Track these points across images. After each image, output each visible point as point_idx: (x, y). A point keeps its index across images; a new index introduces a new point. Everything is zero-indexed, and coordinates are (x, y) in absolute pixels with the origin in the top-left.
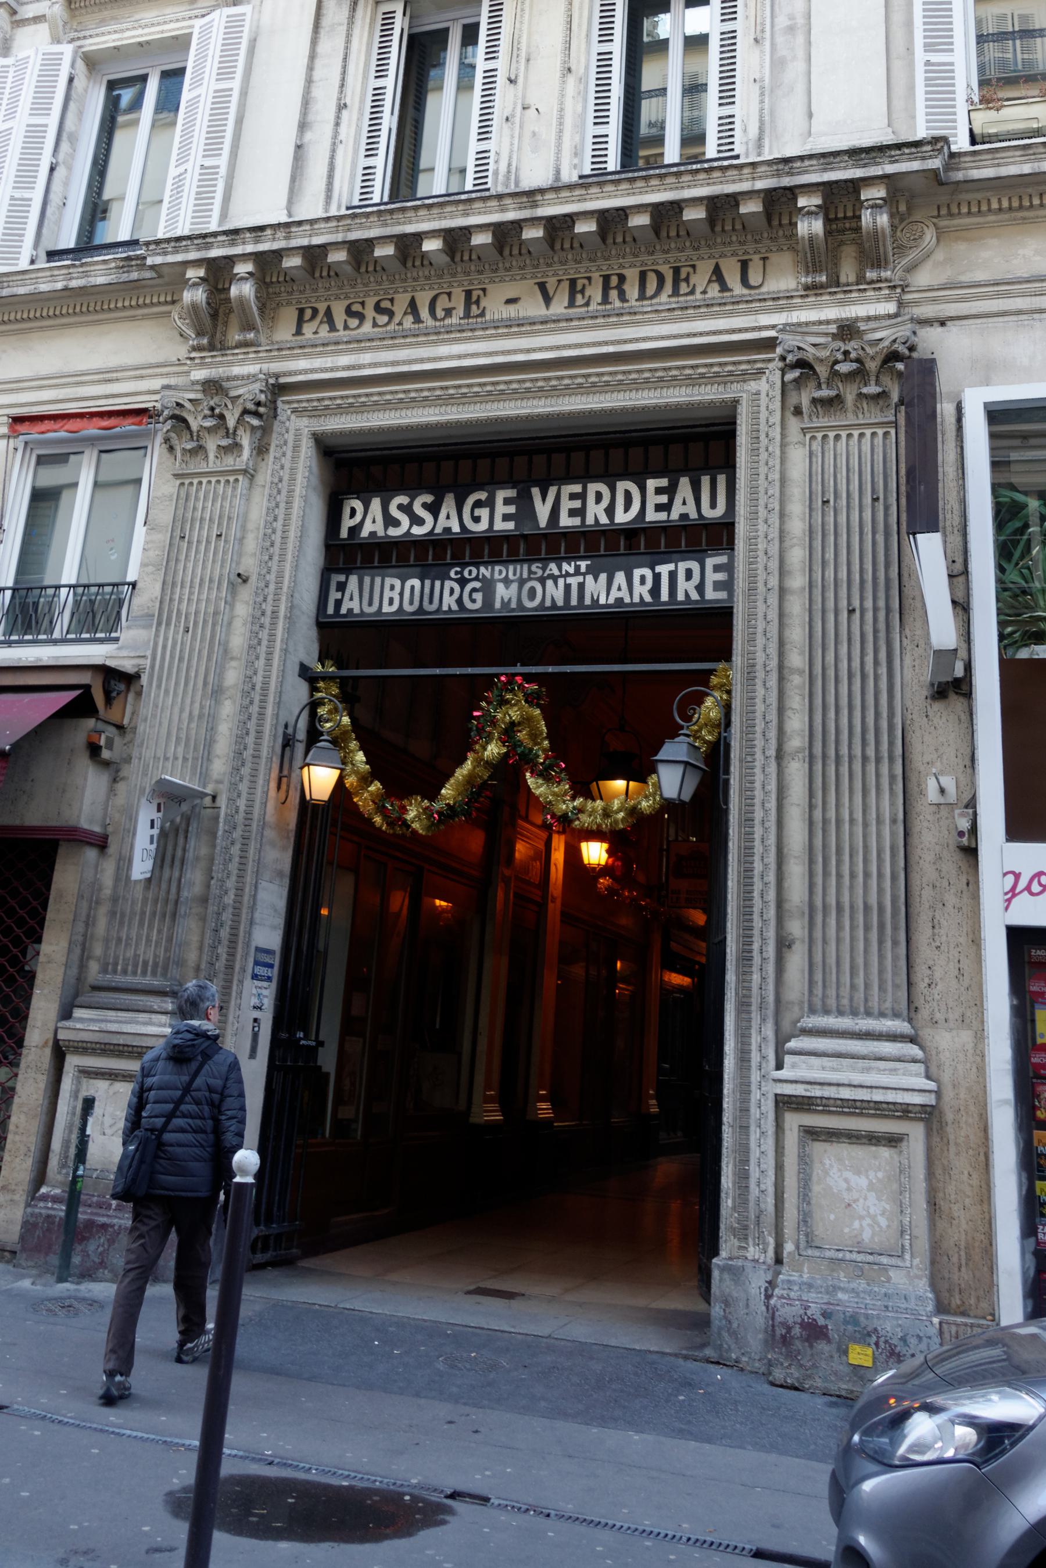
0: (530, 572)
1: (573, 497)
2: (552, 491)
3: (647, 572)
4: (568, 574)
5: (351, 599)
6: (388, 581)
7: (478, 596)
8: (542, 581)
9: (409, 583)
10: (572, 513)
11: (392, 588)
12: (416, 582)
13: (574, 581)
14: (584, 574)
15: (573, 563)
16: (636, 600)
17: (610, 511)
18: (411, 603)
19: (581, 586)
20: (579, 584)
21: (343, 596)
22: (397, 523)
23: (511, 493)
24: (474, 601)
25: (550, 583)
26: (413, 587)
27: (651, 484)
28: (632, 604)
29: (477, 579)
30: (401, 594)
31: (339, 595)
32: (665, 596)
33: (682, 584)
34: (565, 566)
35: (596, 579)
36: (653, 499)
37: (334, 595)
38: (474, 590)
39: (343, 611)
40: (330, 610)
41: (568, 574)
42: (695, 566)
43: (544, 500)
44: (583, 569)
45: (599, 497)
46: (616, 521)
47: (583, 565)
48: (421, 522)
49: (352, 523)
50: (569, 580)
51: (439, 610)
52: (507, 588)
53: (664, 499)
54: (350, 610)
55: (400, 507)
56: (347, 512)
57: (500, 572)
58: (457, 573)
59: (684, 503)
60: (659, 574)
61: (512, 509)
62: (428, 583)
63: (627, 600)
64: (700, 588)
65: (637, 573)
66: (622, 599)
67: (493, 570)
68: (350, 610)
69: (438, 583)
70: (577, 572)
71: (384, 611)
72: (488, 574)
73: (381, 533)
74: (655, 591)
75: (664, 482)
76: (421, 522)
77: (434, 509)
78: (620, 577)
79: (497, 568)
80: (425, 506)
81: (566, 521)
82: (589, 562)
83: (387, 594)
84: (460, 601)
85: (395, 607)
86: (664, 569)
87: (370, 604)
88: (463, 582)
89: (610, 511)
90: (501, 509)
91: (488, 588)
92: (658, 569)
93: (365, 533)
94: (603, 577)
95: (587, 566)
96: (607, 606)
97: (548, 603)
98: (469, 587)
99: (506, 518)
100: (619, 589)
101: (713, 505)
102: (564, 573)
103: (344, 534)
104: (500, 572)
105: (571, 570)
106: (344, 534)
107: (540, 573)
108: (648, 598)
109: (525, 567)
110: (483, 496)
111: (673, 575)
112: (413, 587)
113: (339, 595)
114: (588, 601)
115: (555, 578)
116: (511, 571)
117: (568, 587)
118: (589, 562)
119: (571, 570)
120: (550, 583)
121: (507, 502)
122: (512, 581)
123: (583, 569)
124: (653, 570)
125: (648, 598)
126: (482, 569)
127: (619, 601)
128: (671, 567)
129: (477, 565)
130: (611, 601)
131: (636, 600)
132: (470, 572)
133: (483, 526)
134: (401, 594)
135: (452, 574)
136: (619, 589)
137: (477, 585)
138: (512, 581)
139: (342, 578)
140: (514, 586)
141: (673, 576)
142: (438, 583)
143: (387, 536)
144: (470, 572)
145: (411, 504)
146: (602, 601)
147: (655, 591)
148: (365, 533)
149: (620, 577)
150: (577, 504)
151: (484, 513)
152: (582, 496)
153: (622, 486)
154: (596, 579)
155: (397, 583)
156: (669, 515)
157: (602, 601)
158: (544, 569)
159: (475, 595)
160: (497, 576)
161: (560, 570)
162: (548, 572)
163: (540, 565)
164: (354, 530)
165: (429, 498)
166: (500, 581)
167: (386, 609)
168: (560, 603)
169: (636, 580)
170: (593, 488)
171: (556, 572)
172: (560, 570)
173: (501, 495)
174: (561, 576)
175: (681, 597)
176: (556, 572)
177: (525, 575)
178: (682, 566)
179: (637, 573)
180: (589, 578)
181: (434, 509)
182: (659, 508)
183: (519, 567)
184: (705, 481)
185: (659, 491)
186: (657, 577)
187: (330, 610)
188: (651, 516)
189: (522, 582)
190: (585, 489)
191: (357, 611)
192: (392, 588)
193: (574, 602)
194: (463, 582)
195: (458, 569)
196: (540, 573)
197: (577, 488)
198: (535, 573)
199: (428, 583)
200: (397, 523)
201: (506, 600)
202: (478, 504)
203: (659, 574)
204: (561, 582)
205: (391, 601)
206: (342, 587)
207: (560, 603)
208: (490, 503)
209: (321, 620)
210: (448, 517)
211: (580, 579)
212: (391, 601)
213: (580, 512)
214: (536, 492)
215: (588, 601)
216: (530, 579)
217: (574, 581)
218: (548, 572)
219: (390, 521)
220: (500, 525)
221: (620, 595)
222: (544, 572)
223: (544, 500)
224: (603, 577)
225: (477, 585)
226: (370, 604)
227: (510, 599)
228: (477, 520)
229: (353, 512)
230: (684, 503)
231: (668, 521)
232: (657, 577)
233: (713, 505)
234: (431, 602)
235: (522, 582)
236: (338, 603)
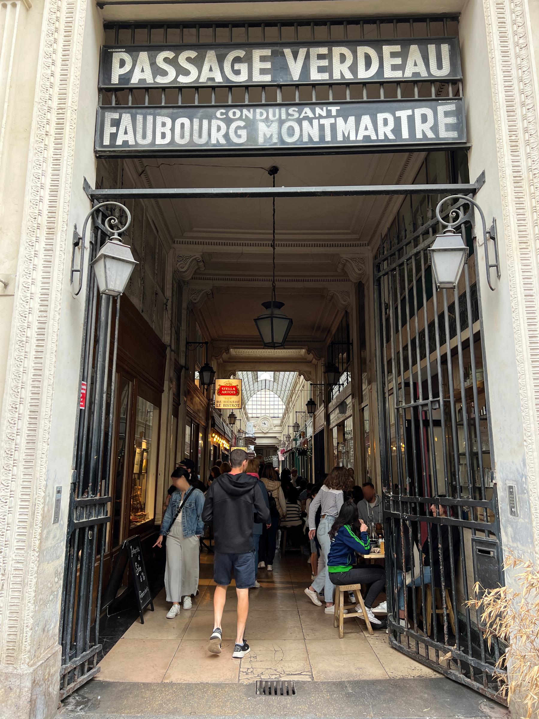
0: (288, 114)
1: (321, 57)
2: (302, 52)
3: (389, 117)
4: (321, 117)
5: (126, 133)
6: (160, 120)
7: (243, 133)
8: (299, 121)
9: (179, 122)
10: (321, 70)
11: (164, 124)
12: (186, 121)
13: (327, 122)
14: (335, 117)
15: (325, 108)
16: (381, 137)
17: (353, 69)
18: (182, 136)
19: (333, 127)
20: (331, 124)
21: (118, 130)
22: (164, 73)
23: (267, 52)
24: (239, 136)
25: (305, 123)
26: (183, 125)
27: (387, 49)
28: (378, 140)
29: (240, 119)
30: (173, 130)
31: (114, 130)
32: (405, 134)
33: (419, 127)
34: (318, 110)
35: (346, 121)
36: (388, 62)
37: (109, 130)
38: (239, 127)
39: (119, 142)
40: (107, 141)
41: (321, 117)
42: (429, 112)
43: (295, 57)
44: (334, 113)
45: (343, 58)
46: (359, 77)
47: (334, 109)
48: (187, 73)
49: (123, 71)
50: (322, 121)
51: (207, 144)
52: (268, 126)
53: (398, 61)
54: (125, 143)
55: (166, 60)
56: (116, 63)
57: (261, 114)
58: (222, 114)
59: (416, 65)
60: (400, 118)
61: (268, 65)
62: (196, 121)
63: (374, 137)
64: (435, 128)
65: (380, 117)
66: (369, 136)
67: (254, 112)
68: (125, 143)
69: (205, 122)
70: (329, 115)
71: (157, 143)
72: (250, 116)
73: (150, 80)
74: (397, 130)
75: (397, 48)
76: (187, 73)
77: (198, 62)
78: (366, 120)
79: (258, 110)
80: (189, 59)
81: (315, 76)
82: (339, 108)
83: (159, 130)
84: (226, 136)
85: (168, 140)
86: (404, 114)
87: (144, 137)
88: (228, 122)
89: (353, 69)
90: (257, 65)
91: (250, 125)
92: (398, 114)
93: (135, 80)
94: (352, 120)
95: (337, 110)
96: (356, 141)
97: (305, 139)
98: (233, 126)
99: (263, 71)
100: (366, 129)
101: (440, 66)
102: (317, 115)
103: (115, 80)
104: (261, 114)
105: (324, 114)
106: (115, 80)
107: (296, 115)
108: (391, 136)
109: (283, 110)
110: (241, 53)
111: (411, 119)
112: (183, 125)
113: (114, 130)
114: (340, 138)
115: (310, 120)
116: (272, 113)
117: (322, 128)
118: (339, 108)
119: (324, 114)
120: (305, 123)
121: (263, 59)
122: (272, 121)
123: (334, 113)
124: (394, 115)
125: (391, 136)
126: (245, 111)
127: (367, 138)
128: (409, 112)
129: (241, 106)
130: (360, 138)
131: (381, 137)
132: (234, 114)
133: (242, 78)
134: (173, 130)
135: (218, 114)
136: (366, 129)
137: (242, 124)
138: (272, 121)
139: (116, 116)
140: (275, 125)
141: (411, 119)
142: (205, 122)
143: (155, 83)
144: (234, 114)
145: (176, 58)
146: (352, 137)
147: (397, 130)
148: (135, 80)
149: (366, 120)
150: (324, 63)
151: (243, 67)
152: (329, 56)
153: (362, 50)
154: (346, 121)
155: (169, 121)
156: (403, 74)
157: (352, 137)
158: (300, 113)
159: (240, 132)
160: (258, 117)
161: (314, 112)
162: (303, 115)
163: (297, 110)
164: (125, 78)
165: (193, 54)
166: (262, 121)
167: (159, 141)
168: (316, 139)
169: (380, 122)
170: (337, 51)
171: (311, 115)
172: (314, 112)
173: (257, 53)
174: (315, 118)
175: (419, 135)
176: (311, 115)
177: (284, 117)
178: (419, 112)
179: (380, 117)
180: (340, 120)
181: (198, 62)
182: (394, 68)
183: (277, 111)
184: (432, 48)
185: (393, 55)
186: (398, 121)
187: (107, 141)
188: (389, 74)
189: (281, 122)
190: (330, 51)
191: (132, 142)
192: (164, 124)
193: (328, 138)
194: (228, 122)
195: (224, 111)
196: (296, 115)
197: (324, 50)
198: (293, 115)
199: (196, 121)
200: (164, 73)
201: (268, 136)
202: (237, 60)
203: (400, 118)
204: (315, 122)
205: (163, 136)
206: (116, 123)
207: (316, 139)
208: (248, 60)
209: (98, 149)
210: (211, 70)
211: (332, 120)
212: (163, 136)
213: (328, 69)
214: (288, 52)
215: (340, 138)
216: (287, 120)
217: (327, 122)
218: (303, 115)
219: (157, 71)
220: (258, 78)
221: (367, 133)
222: (300, 115)
223: (295, 57)
224: (352, 120)
225: (242, 124)
226: (144, 137)
227: (272, 135)
228: (237, 73)
229: (122, 63)
230: (416, 65)
231: (403, 77)
232: (398, 121)
233: (440, 66)
234: (200, 136)
235: (281, 122)
236: (114, 136)
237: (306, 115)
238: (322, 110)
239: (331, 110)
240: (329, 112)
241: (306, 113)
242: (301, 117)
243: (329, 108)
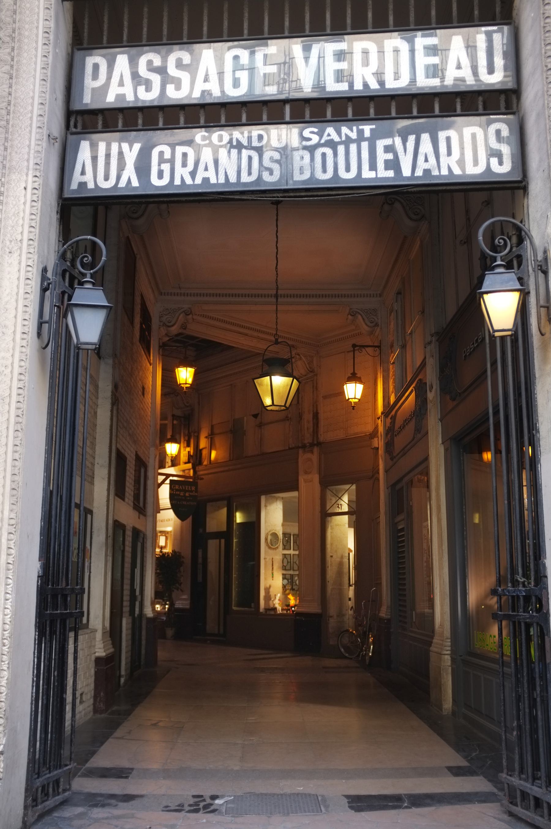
15: (355, 128)
34: (345, 130)
44: (367, 134)
47: (367, 129)
82: (374, 127)
95: (371, 130)
102: (344, 138)
105: (354, 135)
118: (374, 127)
119: (354, 135)
123: (367, 134)
161: (339, 133)
162: (325, 138)
163: (316, 130)
171: (336, 139)
196: (315, 139)
222: (321, 137)
237: (329, 138)
238: (352, 130)
239: (363, 131)
240: (361, 133)
241: (329, 135)
242: (323, 141)
243: (361, 127)
